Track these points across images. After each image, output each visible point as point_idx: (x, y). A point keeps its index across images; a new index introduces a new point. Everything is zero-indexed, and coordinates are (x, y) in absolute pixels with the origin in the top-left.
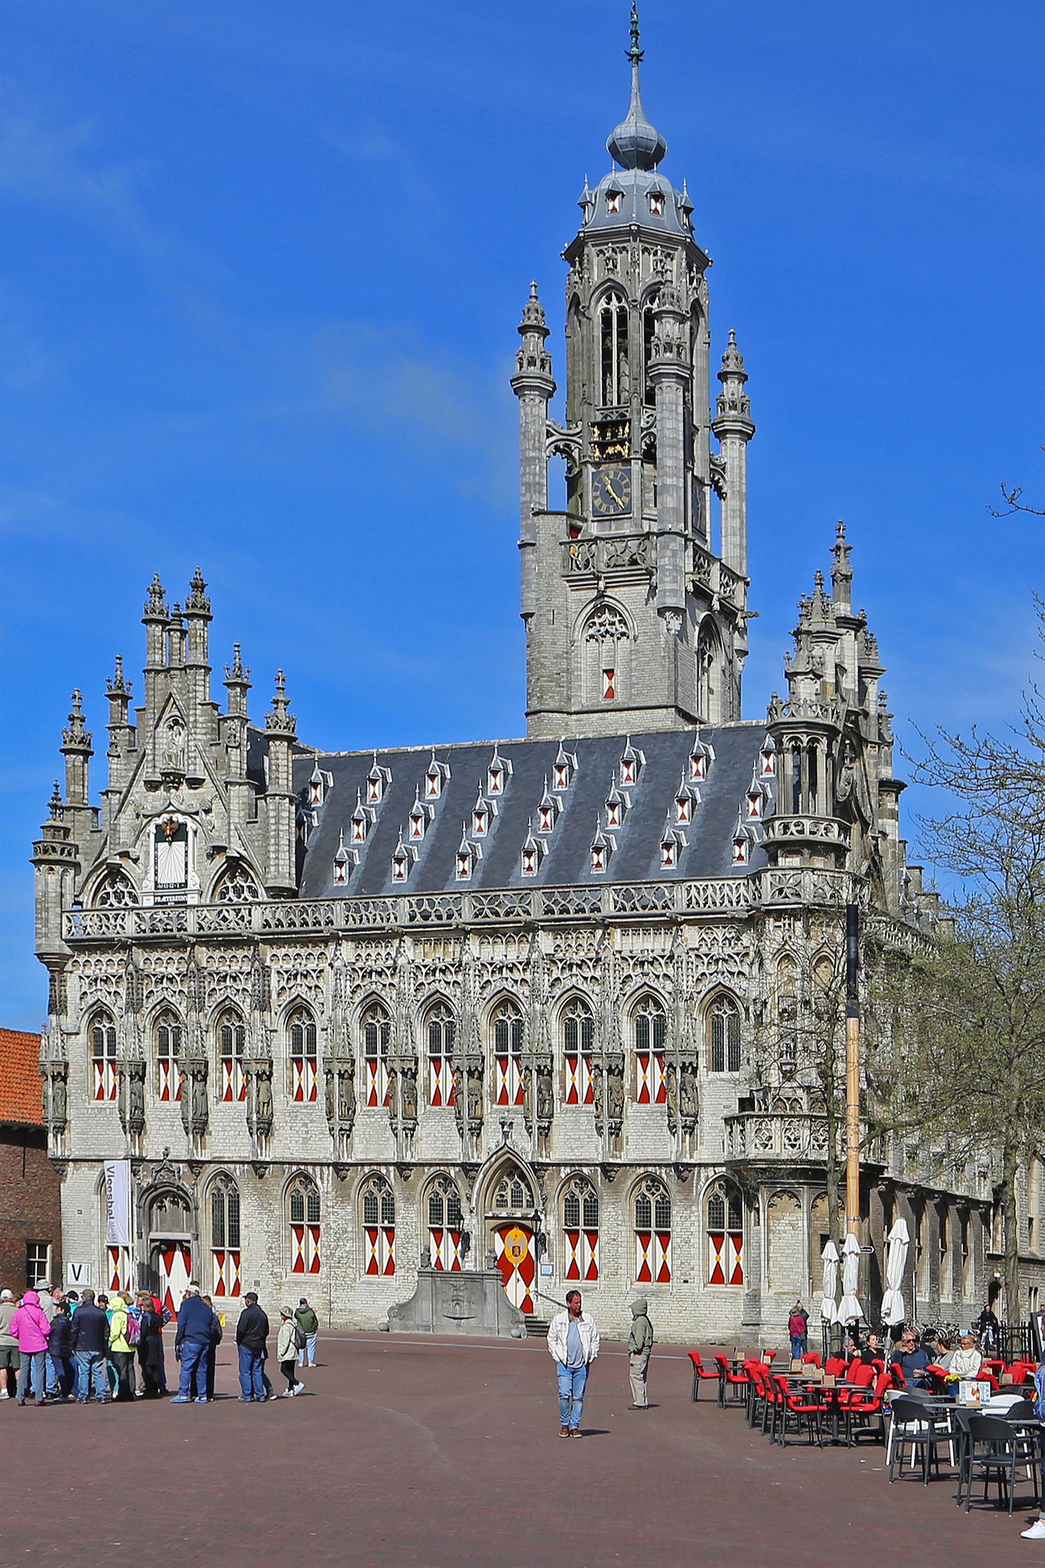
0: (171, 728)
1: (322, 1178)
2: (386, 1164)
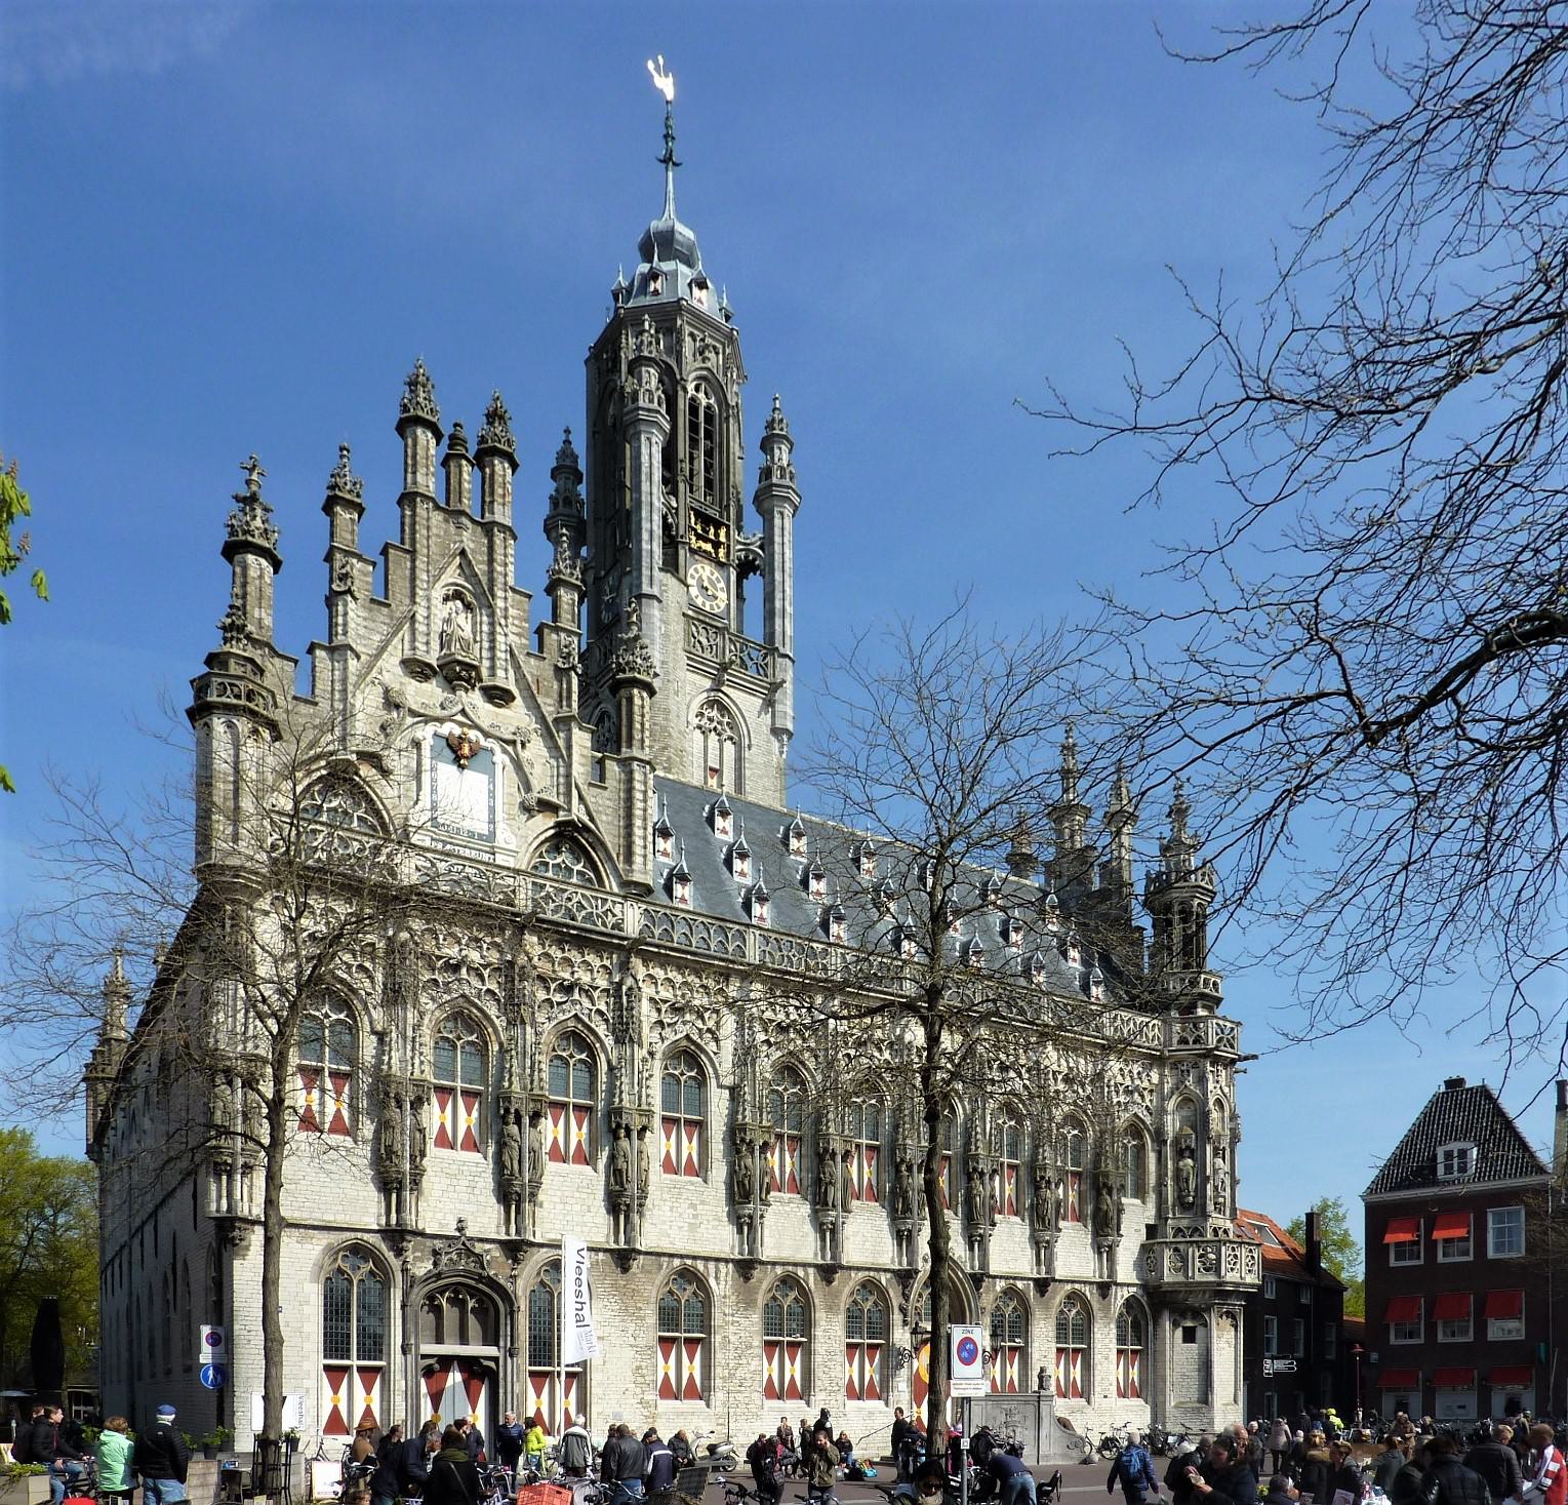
1: (717, 1278)
2: (805, 1265)
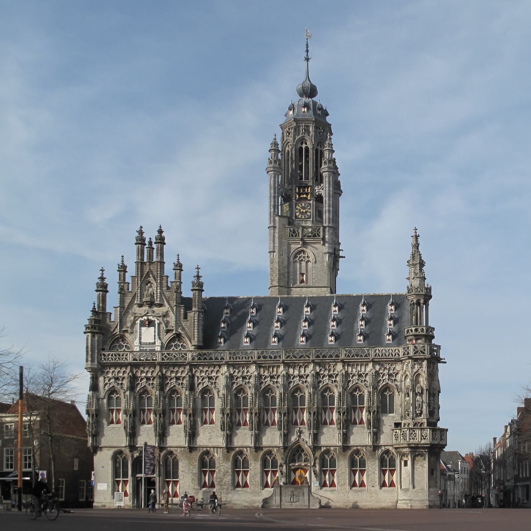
0: (147, 284)
1: (217, 453)
2: (246, 447)
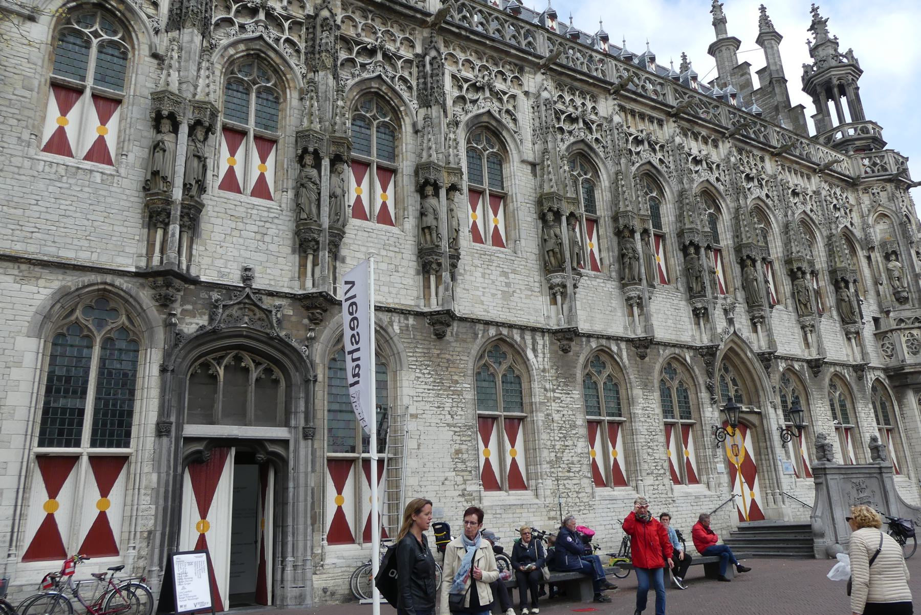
1: (534, 350)
2: (617, 339)
